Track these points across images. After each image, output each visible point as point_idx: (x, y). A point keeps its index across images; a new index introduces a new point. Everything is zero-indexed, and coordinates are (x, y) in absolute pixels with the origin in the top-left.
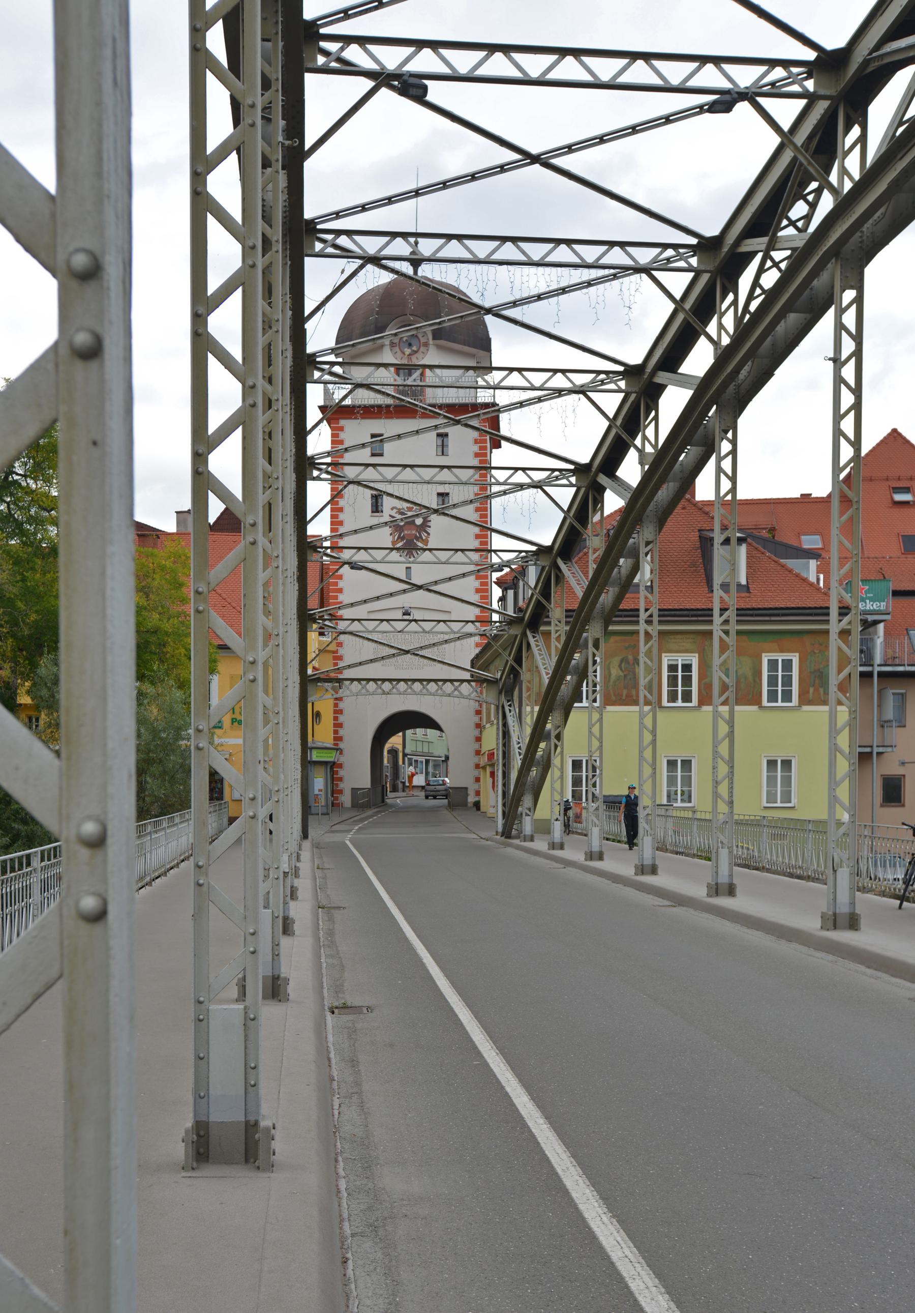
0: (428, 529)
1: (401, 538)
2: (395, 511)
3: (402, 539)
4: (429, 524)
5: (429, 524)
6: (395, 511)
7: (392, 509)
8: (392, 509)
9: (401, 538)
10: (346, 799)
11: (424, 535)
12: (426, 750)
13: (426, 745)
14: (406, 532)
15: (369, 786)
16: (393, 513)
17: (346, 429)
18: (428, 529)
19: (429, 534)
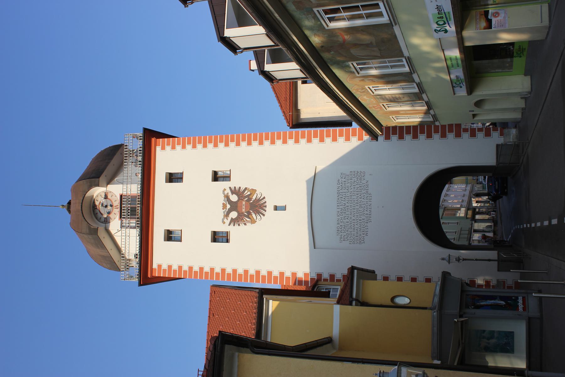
1: (249, 215)
2: (225, 220)
3: (249, 213)
4: (237, 188)
5: (237, 188)
6: (225, 220)
7: (224, 223)
8: (224, 223)
9: (249, 215)
10: (511, 277)
11: (247, 193)
12: (467, 232)
13: (463, 232)
14: (244, 210)
15: (496, 252)
16: (227, 221)
17: (160, 263)
18: (242, 189)
19: (246, 189)
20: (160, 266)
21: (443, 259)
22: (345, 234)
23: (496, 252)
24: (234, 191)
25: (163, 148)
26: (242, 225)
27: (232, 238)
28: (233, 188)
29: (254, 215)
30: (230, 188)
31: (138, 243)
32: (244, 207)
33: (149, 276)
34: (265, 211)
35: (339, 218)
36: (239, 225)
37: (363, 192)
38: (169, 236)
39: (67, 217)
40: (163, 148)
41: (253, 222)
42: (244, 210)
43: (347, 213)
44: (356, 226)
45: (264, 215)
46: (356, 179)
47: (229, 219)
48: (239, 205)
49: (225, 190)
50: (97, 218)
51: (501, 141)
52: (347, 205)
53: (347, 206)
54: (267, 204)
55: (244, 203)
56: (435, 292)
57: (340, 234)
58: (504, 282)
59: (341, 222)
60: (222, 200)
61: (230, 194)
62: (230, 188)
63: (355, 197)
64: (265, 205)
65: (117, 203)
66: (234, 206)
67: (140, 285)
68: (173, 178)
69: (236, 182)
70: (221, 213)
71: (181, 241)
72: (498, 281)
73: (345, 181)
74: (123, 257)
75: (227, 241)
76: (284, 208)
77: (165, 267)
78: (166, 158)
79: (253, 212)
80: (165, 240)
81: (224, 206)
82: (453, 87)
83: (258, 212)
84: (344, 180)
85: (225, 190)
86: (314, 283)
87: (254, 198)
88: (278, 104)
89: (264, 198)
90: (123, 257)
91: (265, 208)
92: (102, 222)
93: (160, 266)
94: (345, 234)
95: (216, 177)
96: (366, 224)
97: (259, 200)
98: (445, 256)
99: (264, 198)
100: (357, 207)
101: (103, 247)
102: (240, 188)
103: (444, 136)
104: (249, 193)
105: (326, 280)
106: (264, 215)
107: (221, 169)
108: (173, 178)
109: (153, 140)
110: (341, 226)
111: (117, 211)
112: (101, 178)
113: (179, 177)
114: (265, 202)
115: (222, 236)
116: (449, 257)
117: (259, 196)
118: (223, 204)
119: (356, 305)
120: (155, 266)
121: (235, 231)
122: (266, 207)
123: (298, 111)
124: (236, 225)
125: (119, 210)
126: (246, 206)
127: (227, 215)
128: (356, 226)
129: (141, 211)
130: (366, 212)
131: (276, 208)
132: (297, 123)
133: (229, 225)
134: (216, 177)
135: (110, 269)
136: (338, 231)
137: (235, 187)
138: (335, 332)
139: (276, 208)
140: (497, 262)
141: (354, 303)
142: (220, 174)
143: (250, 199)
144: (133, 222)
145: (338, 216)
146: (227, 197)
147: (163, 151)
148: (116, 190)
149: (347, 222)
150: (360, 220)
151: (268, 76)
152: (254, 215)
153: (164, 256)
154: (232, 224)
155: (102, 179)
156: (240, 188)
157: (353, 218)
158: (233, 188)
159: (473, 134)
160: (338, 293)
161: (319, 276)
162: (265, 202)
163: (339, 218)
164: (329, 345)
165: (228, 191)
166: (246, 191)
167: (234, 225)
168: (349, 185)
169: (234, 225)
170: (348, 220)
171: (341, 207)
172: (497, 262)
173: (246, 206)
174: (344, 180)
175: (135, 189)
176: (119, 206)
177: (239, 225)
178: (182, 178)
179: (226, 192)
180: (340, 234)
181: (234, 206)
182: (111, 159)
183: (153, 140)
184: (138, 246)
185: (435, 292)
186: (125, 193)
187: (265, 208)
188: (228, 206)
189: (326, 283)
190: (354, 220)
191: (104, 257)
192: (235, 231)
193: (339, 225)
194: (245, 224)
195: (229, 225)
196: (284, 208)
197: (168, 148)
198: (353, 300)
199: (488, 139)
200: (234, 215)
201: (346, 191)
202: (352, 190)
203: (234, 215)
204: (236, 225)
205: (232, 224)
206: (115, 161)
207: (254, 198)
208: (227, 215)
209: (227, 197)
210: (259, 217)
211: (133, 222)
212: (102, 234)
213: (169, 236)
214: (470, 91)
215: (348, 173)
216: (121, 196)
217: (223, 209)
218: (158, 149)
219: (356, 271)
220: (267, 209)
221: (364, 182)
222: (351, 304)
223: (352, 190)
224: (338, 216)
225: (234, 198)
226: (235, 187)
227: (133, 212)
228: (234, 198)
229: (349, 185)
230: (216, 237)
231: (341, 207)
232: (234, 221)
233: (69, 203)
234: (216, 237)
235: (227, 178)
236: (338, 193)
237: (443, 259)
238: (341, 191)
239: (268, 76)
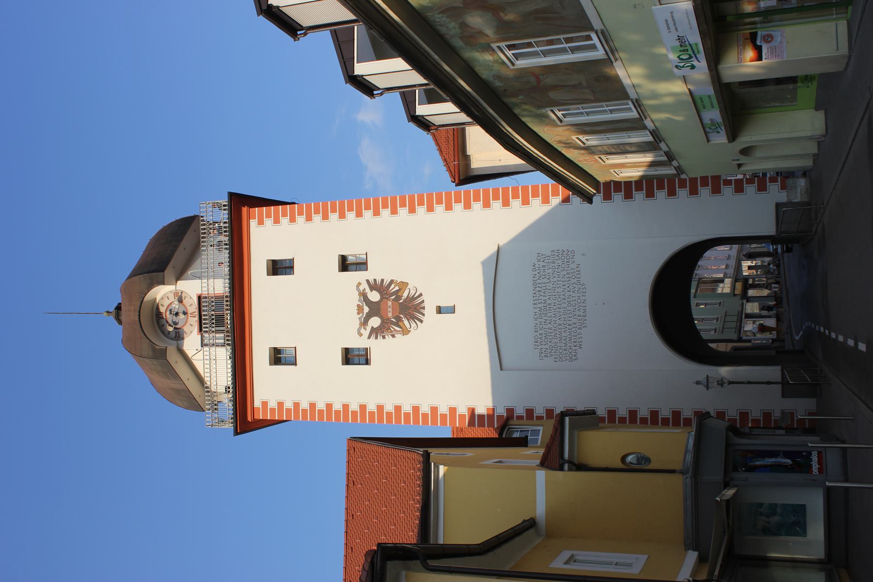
0: (386, 283)
1: (398, 322)
2: (362, 331)
3: (399, 319)
6: (362, 331)
7: (361, 335)
8: (361, 335)
9: (398, 322)
10: (802, 407)
11: (394, 288)
14: (390, 315)
15: (779, 368)
16: (366, 333)
17: (265, 399)
18: (386, 283)
19: (392, 282)
20: (265, 404)
21: (698, 383)
22: (547, 347)
23: (779, 368)
24: (374, 286)
25: (261, 222)
26: (389, 338)
27: (374, 357)
28: (372, 282)
29: (406, 322)
30: (368, 281)
31: (230, 370)
32: (390, 310)
33: (249, 419)
34: (424, 315)
35: (537, 322)
36: (384, 337)
37: (573, 281)
38: (277, 357)
39: (118, 330)
40: (261, 222)
41: (405, 332)
42: (390, 315)
43: (549, 315)
44: (564, 334)
45: (421, 321)
46: (561, 263)
47: (369, 328)
48: (382, 307)
49: (359, 284)
50: (163, 333)
51: (783, 197)
52: (549, 301)
53: (549, 304)
54: (425, 304)
55: (390, 303)
56: (687, 447)
57: (540, 347)
58: (792, 414)
59: (541, 329)
60: (355, 299)
61: (368, 290)
62: (368, 281)
63: (560, 290)
64: (422, 305)
65: (193, 308)
66: (375, 309)
67: (236, 433)
68: (278, 268)
69: (376, 272)
70: (355, 320)
71: (296, 364)
72: (783, 412)
73: (544, 266)
74: (208, 392)
75: (367, 362)
76: (452, 310)
77: (272, 404)
78: (266, 238)
79: (405, 317)
80: (270, 364)
81: (360, 309)
82: (706, 133)
83: (412, 317)
84: (542, 264)
85: (359, 284)
86: (502, 422)
87: (405, 295)
88: (435, 148)
89: (421, 295)
90: (208, 392)
91: (422, 311)
92: (172, 339)
93: (265, 404)
94: (547, 347)
95: (345, 265)
96: (578, 331)
97: (414, 298)
98: (702, 378)
99: (421, 295)
100: (563, 305)
101: (176, 376)
102: (382, 280)
103: (694, 192)
104: (397, 288)
105: (520, 418)
106: (421, 321)
107: (353, 252)
108: (278, 268)
109: (245, 210)
110: (541, 334)
111: (194, 321)
112: (166, 272)
113: (287, 265)
114: (423, 301)
115: (359, 355)
116: (708, 380)
117: (413, 292)
118: (358, 306)
119: (570, 470)
120: (257, 404)
121: (378, 348)
122: (424, 308)
123: (467, 158)
124: (380, 338)
125: (197, 319)
126: (393, 308)
127: (364, 323)
128: (564, 334)
129: (232, 318)
130: (578, 313)
131: (440, 310)
132: (465, 175)
133: (369, 337)
134: (345, 265)
135: (187, 408)
136: (536, 342)
137: (375, 280)
138: (540, 510)
139: (440, 310)
140: (780, 386)
141: (566, 466)
142: (351, 259)
143: (398, 298)
144: (220, 338)
145: (536, 319)
146: (364, 295)
147: (261, 228)
148: (191, 288)
149: (550, 329)
150: (570, 325)
151: (423, 123)
152: (406, 322)
153: (270, 387)
154: (373, 336)
155: (169, 272)
156: (382, 280)
157: (559, 322)
158: (372, 282)
159: (739, 187)
160: (540, 437)
161: (510, 411)
162: (423, 301)
163: (537, 322)
164: (532, 531)
165: (365, 286)
166: (393, 286)
167: (376, 338)
168: (550, 271)
169: (376, 338)
170: (550, 326)
171: (539, 306)
172: (780, 386)
173: (393, 308)
174: (542, 264)
175: (220, 286)
176: (197, 313)
177: (384, 337)
178: (292, 268)
179: (361, 288)
180: (540, 347)
181: (375, 309)
182: (180, 240)
183: (245, 210)
184: (230, 375)
185: (687, 447)
186: (205, 293)
187: (422, 311)
188: (366, 309)
189: (520, 422)
190: (560, 325)
191: (178, 391)
192: (378, 348)
193: (537, 334)
194: (393, 336)
195: (369, 337)
196: (452, 310)
197: (269, 222)
198: (565, 461)
199: (763, 195)
200: (375, 322)
201: (545, 280)
202: (555, 279)
203: (375, 322)
204: (380, 338)
205: (373, 336)
206: (187, 242)
207: (405, 295)
208: (364, 323)
209: (364, 295)
210: (413, 325)
211: (220, 338)
212: (173, 357)
213: (277, 357)
214: (733, 136)
215: (549, 253)
216: (199, 298)
217: (358, 314)
218: (253, 223)
219: (567, 419)
220: (425, 312)
221: (573, 266)
222: (561, 469)
223: (555, 279)
224: (536, 319)
225: (374, 296)
226: (375, 280)
227: (219, 321)
228: (374, 296)
229: (550, 271)
230: (349, 357)
231: (539, 306)
232: (375, 332)
233: (119, 308)
234: (349, 357)
235: (362, 265)
236: (535, 284)
237: (698, 383)
238: (538, 281)
239: (423, 123)
